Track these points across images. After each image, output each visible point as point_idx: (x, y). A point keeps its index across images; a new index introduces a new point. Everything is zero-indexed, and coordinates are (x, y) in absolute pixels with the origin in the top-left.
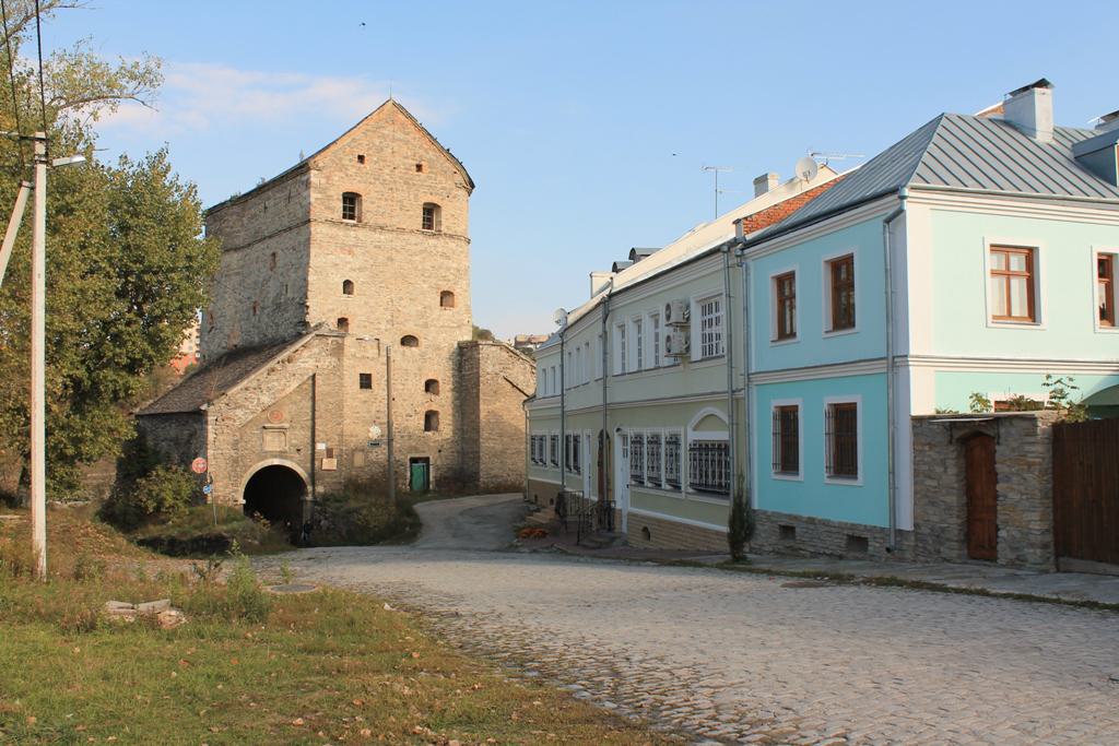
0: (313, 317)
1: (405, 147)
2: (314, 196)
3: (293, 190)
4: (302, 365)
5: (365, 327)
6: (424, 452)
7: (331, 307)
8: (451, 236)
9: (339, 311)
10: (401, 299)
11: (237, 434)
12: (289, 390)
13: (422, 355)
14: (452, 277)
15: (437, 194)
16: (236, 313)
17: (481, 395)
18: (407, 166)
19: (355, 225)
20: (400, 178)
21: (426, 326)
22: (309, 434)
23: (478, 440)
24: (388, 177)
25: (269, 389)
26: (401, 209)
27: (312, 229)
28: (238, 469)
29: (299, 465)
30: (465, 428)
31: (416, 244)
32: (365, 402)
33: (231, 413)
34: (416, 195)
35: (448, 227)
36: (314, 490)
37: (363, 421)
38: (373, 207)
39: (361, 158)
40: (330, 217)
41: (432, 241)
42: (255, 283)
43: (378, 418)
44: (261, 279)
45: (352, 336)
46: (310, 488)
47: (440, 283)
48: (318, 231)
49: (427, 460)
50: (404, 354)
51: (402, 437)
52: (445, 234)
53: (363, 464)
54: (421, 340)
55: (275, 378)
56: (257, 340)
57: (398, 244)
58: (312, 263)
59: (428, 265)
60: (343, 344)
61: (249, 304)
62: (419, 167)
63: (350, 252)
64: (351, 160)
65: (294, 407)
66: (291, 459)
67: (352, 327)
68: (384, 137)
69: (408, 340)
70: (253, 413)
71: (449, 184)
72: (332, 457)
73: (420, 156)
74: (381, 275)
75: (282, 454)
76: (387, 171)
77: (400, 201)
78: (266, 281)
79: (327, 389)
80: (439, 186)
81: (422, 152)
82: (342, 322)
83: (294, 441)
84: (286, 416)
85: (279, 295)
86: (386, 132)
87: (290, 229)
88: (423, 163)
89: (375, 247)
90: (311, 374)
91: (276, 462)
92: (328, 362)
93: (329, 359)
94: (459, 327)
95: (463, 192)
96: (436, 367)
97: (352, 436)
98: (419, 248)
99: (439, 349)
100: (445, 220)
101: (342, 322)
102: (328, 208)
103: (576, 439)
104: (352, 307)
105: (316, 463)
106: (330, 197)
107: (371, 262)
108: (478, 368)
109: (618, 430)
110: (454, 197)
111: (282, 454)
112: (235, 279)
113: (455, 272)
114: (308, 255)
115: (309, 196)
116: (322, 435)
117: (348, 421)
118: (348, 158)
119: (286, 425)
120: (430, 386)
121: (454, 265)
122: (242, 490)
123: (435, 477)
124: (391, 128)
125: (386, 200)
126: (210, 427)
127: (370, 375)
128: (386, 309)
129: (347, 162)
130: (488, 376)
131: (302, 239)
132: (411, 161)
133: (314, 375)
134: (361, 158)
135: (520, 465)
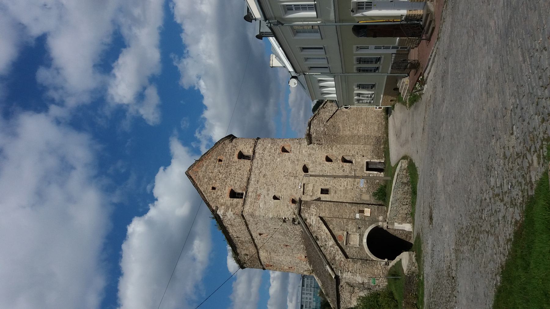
4: (314, 222)
7: (286, 207)
8: (255, 146)
10: (284, 172)
12: (327, 231)
13: (313, 162)
14: (275, 147)
15: (234, 152)
19: (246, 193)
20: (225, 169)
21: (298, 160)
26: (240, 170)
31: (258, 163)
32: (335, 192)
34: (234, 162)
35: (250, 148)
37: (345, 194)
38: (238, 183)
41: (257, 155)
49: (367, 163)
55: (320, 237)
56: (302, 246)
57: (257, 172)
62: (220, 160)
64: (214, 193)
65: (336, 229)
66: (364, 232)
68: (204, 176)
71: (230, 146)
73: (215, 159)
74: (272, 181)
75: (361, 236)
76: (220, 176)
79: (327, 211)
80: (230, 151)
81: (212, 159)
82: (294, 201)
83: (354, 230)
84: (340, 233)
85: (280, 233)
86: (201, 176)
88: (218, 158)
91: (365, 240)
93: (312, 209)
94: (300, 144)
98: (260, 162)
100: (247, 151)
101: (294, 201)
102: (237, 206)
103: (360, 61)
104: (286, 194)
106: (231, 204)
107: (265, 185)
109: (353, 11)
110: (236, 144)
111: (361, 236)
112: (273, 254)
119: (345, 233)
120: (328, 159)
123: (377, 159)
124: (200, 173)
125: (235, 177)
128: (289, 179)
129: (215, 195)
134: (214, 188)
135: (373, 115)
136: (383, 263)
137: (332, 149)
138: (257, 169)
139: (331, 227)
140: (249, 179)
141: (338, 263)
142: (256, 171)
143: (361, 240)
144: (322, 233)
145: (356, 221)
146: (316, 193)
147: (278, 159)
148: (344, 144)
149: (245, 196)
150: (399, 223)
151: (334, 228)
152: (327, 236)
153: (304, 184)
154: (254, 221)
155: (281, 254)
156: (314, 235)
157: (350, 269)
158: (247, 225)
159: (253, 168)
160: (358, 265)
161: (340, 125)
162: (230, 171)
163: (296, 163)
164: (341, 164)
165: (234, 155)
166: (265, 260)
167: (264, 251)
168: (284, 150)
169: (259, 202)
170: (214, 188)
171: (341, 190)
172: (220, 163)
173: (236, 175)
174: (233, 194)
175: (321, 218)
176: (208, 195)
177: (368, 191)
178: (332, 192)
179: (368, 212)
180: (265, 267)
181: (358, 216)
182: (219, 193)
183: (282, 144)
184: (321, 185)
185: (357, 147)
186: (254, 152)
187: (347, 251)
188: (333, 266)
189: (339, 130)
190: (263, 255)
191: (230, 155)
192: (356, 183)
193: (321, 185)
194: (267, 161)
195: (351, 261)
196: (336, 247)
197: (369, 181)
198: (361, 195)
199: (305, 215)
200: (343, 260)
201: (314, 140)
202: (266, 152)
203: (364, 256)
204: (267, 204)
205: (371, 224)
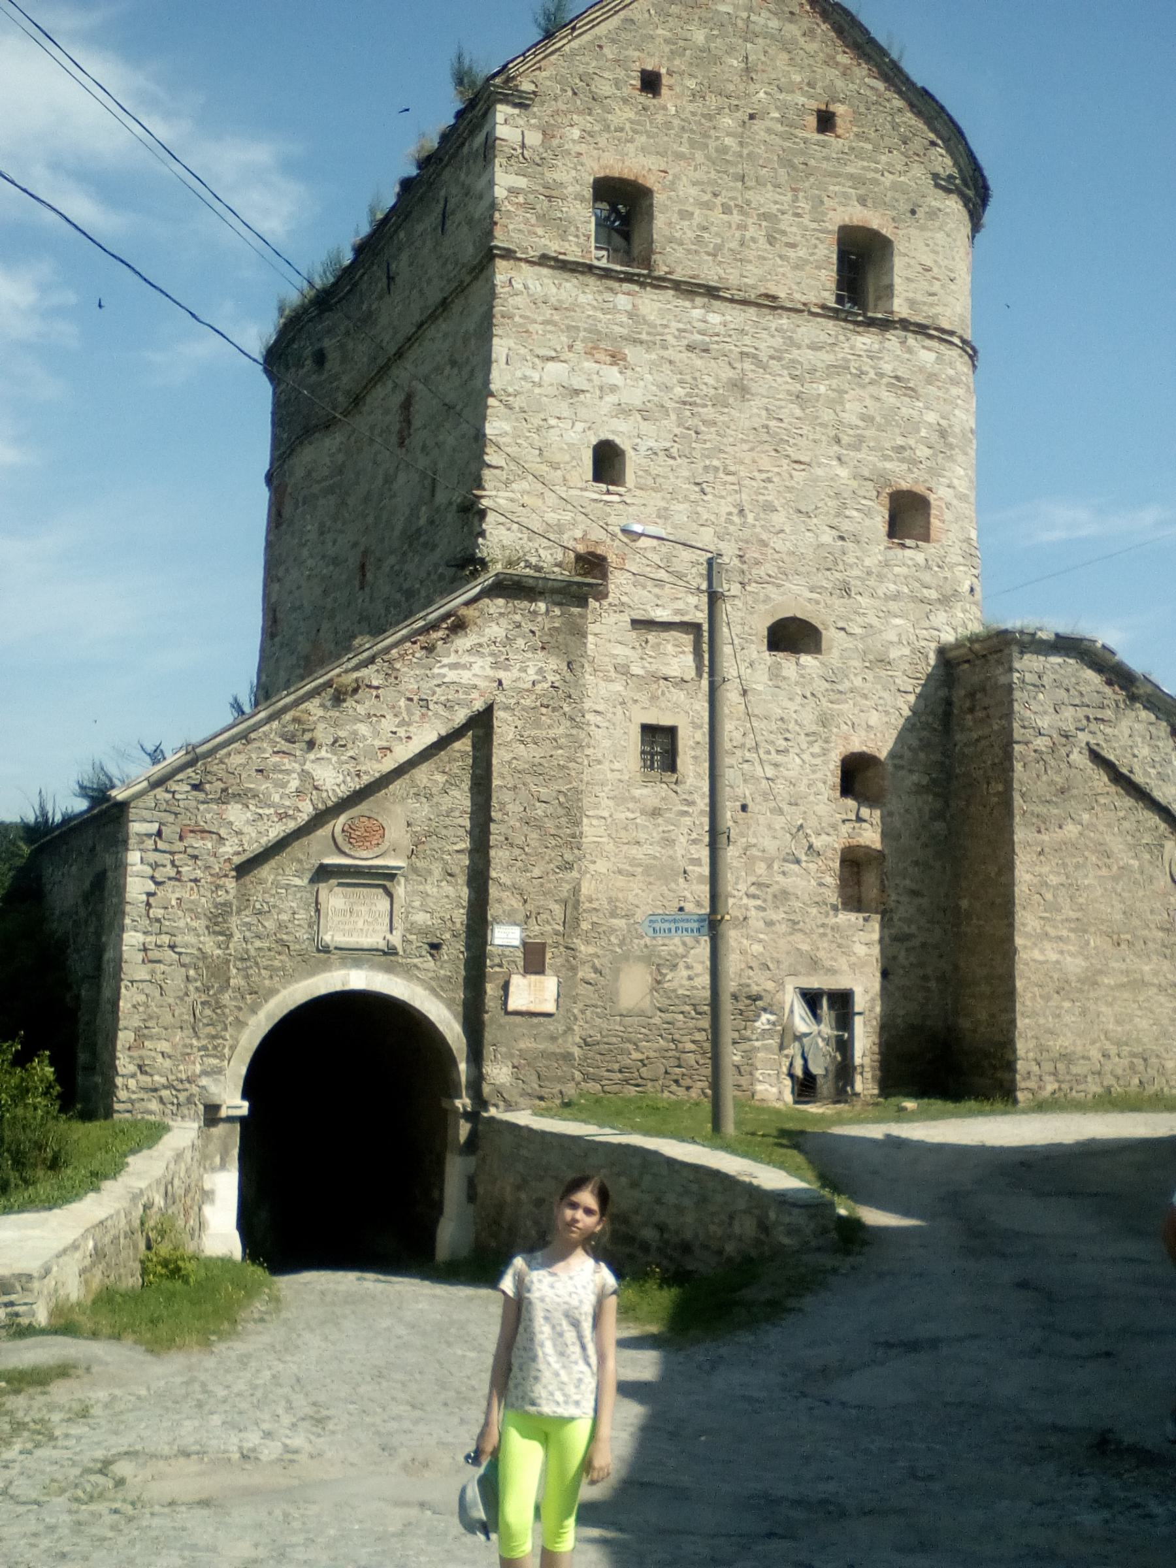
0: (499, 540)
1: (785, 56)
2: (505, 180)
3: (454, 192)
5: (659, 583)
6: (832, 971)
8: (921, 330)
9: (579, 534)
10: (769, 508)
12: (404, 752)
14: (922, 452)
15: (880, 203)
16: (325, 592)
17: (1018, 801)
18: (791, 115)
23: (1010, 939)
24: (729, 141)
26: (771, 240)
27: (500, 278)
28: (226, 998)
29: (433, 991)
30: (964, 904)
31: (814, 347)
32: (655, 813)
33: (207, 815)
35: (912, 303)
38: (686, 231)
40: (553, 247)
42: (367, 499)
44: (379, 481)
45: (621, 607)
47: (888, 465)
48: (518, 287)
50: (775, 673)
51: (770, 924)
52: (905, 324)
53: (646, 1004)
54: (830, 635)
55: (361, 709)
57: (766, 344)
58: (499, 377)
59: (851, 412)
61: (353, 561)
62: (826, 122)
63: (616, 358)
64: (617, 84)
65: (423, 810)
66: (408, 971)
67: (618, 583)
70: (282, 817)
72: (541, 971)
74: (709, 434)
77: (765, 216)
78: (389, 480)
81: (833, 73)
83: (421, 918)
84: (396, 833)
85: (414, 512)
87: (445, 304)
88: (839, 109)
89: (690, 348)
90: (479, 705)
91: (358, 979)
92: (533, 670)
95: (953, 205)
96: (874, 718)
97: (613, 915)
98: (827, 357)
99: (883, 661)
105: (489, 988)
106: (552, 193)
107: (679, 391)
108: (1009, 715)
110: (933, 214)
111: (386, 956)
113: (934, 438)
114: (487, 362)
115: (491, 183)
117: (601, 866)
118: (606, 74)
121: (931, 417)
122: (238, 1068)
125: (726, 210)
126: (134, 857)
127: (671, 731)
130: (1041, 743)
131: (471, 325)
132: (802, 100)
133: (489, 710)
134: (650, 83)
135: (1144, 1024)
138: (778, 341)
140: (712, 292)
141: (207, 815)
143: (355, 956)
149: (607, 274)
150: (471, 1184)
154: (466, 340)
155: (331, 550)
157: (172, 893)
158: (445, 304)
159: (784, 321)
161: (1071, 829)
162: (760, 182)
165: (862, 201)
166: (300, 472)
167: (341, 457)
170: (650, 83)
171: (668, 842)
172: (812, 121)
173: (736, 218)
176: (609, 52)
179: (531, 993)
180: (275, 483)
182: (623, 115)
186: (885, 325)
187: (286, 879)
188: (181, 788)
189: (1041, 824)
190: (321, 452)
191: (858, 181)
194: (831, 404)
195: (222, 896)
196: (306, 810)
199: (496, 621)
200: (228, 849)
202: (890, 399)
204: (563, 408)
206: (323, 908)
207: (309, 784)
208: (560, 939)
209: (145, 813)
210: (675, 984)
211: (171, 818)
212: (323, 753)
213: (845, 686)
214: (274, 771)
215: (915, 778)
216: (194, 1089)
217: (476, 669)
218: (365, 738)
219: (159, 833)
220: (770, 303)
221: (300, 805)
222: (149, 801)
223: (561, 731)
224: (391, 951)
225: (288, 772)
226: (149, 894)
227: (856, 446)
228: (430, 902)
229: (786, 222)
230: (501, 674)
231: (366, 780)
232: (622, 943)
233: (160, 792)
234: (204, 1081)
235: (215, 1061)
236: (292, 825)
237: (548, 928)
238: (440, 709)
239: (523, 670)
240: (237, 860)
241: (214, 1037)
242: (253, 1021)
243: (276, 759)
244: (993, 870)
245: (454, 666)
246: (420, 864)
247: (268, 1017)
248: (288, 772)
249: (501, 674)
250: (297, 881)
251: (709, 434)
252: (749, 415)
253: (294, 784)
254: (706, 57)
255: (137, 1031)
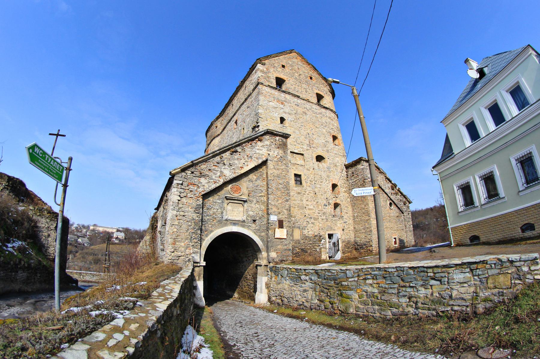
4: (258, 151)
6: (334, 230)
11: (201, 200)
13: (328, 168)
14: (335, 130)
22: (263, 207)
25: (230, 165)
29: (255, 233)
32: (299, 193)
34: (312, 89)
36: (268, 255)
37: (298, 207)
39: (283, 66)
43: (307, 205)
46: (264, 254)
51: (323, 219)
54: (326, 159)
55: (236, 157)
60: (286, 142)
62: (311, 78)
65: (251, 185)
69: (320, 158)
74: (301, 119)
75: (242, 223)
79: (276, 172)
83: (251, 213)
84: (244, 190)
87: (246, 100)
89: (296, 105)
90: (264, 159)
92: (276, 153)
93: (277, 151)
102: (268, 81)
106: (269, 77)
111: (242, 223)
116: (274, 209)
119: (245, 197)
133: (267, 160)
136: (197, 258)
137: (345, 192)
139: (252, 176)
140: (298, 97)
141: (196, 180)
142: (308, 105)
143: (235, 223)
144: (243, 161)
145: (266, 216)
146: (294, 168)
147: (324, 130)
148: (353, 206)
151: (251, 181)
152: (238, 167)
153: (302, 155)
156: (239, 149)
157: (184, 200)
158: (246, 100)
160: (191, 214)
163: (325, 149)
164: (332, 202)
168: (335, 138)
169: (275, 102)
171: (302, 200)
174: (280, 82)
175: (265, 163)
177: (305, 238)
178: (298, 189)
179: (281, 233)
181: (274, 218)
183: (339, 136)
184: (305, 175)
185: (351, 221)
188: (189, 172)
191: (318, 87)
192: (312, 221)
193: (305, 175)
196: (221, 181)
197: (317, 238)
198: (299, 228)
199: (267, 140)
200: (200, 190)
201: (351, 170)
202: (329, 120)
203: (208, 226)
204: (274, 110)
205: (262, 240)
206: (226, 208)
207: (222, 174)
208: (287, 219)
209: (180, 179)
210: (305, 233)
211: (186, 180)
212: (226, 167)
213: (331, 170)
214: (214, 170)
215: (344, 189)
216: (191, 257)
217: (263, 150)
218: (236, 164)
219: (182, 184)
220: (308, 101)
221: (220, 180)
222: (180, 175)
223: (283, 167)
224: (244, 221)
225: (217, 171)
226: (179, 200)
227: (326, 126)
228: (253, 209)
229: (308, 90)
230: (269, 152)
231: (237, 175)
232: (294, 224)
233: (183, 174)
234: (193, 255)
235: (196, 249)
236: (218, 185)
237: (283, 216)
238: (255, 159)
239: (274, 152)
240: (203, 193)
241: (197, 243)
242: (206, 239)
243: (214, 167)
244: (363, 206)
245: (258, 149)
246: (251, 199)
247: (211, 239)
248: (217, 171)
249: (269, 152)
250: (219, 201)
251: (301, 119)
252: (308, 117)
253: (219, 174)
254: (291, 66)
255: (174, 239)
